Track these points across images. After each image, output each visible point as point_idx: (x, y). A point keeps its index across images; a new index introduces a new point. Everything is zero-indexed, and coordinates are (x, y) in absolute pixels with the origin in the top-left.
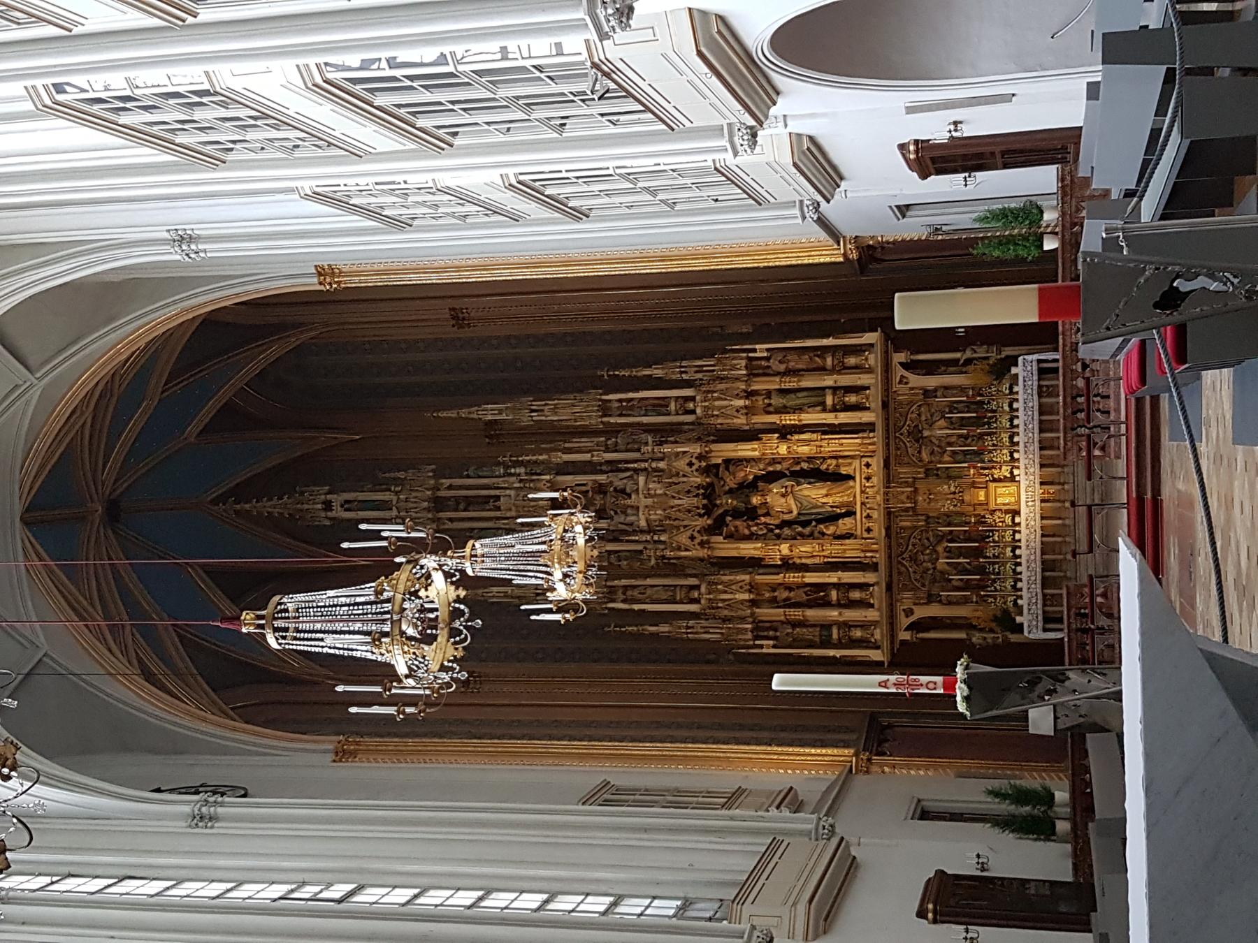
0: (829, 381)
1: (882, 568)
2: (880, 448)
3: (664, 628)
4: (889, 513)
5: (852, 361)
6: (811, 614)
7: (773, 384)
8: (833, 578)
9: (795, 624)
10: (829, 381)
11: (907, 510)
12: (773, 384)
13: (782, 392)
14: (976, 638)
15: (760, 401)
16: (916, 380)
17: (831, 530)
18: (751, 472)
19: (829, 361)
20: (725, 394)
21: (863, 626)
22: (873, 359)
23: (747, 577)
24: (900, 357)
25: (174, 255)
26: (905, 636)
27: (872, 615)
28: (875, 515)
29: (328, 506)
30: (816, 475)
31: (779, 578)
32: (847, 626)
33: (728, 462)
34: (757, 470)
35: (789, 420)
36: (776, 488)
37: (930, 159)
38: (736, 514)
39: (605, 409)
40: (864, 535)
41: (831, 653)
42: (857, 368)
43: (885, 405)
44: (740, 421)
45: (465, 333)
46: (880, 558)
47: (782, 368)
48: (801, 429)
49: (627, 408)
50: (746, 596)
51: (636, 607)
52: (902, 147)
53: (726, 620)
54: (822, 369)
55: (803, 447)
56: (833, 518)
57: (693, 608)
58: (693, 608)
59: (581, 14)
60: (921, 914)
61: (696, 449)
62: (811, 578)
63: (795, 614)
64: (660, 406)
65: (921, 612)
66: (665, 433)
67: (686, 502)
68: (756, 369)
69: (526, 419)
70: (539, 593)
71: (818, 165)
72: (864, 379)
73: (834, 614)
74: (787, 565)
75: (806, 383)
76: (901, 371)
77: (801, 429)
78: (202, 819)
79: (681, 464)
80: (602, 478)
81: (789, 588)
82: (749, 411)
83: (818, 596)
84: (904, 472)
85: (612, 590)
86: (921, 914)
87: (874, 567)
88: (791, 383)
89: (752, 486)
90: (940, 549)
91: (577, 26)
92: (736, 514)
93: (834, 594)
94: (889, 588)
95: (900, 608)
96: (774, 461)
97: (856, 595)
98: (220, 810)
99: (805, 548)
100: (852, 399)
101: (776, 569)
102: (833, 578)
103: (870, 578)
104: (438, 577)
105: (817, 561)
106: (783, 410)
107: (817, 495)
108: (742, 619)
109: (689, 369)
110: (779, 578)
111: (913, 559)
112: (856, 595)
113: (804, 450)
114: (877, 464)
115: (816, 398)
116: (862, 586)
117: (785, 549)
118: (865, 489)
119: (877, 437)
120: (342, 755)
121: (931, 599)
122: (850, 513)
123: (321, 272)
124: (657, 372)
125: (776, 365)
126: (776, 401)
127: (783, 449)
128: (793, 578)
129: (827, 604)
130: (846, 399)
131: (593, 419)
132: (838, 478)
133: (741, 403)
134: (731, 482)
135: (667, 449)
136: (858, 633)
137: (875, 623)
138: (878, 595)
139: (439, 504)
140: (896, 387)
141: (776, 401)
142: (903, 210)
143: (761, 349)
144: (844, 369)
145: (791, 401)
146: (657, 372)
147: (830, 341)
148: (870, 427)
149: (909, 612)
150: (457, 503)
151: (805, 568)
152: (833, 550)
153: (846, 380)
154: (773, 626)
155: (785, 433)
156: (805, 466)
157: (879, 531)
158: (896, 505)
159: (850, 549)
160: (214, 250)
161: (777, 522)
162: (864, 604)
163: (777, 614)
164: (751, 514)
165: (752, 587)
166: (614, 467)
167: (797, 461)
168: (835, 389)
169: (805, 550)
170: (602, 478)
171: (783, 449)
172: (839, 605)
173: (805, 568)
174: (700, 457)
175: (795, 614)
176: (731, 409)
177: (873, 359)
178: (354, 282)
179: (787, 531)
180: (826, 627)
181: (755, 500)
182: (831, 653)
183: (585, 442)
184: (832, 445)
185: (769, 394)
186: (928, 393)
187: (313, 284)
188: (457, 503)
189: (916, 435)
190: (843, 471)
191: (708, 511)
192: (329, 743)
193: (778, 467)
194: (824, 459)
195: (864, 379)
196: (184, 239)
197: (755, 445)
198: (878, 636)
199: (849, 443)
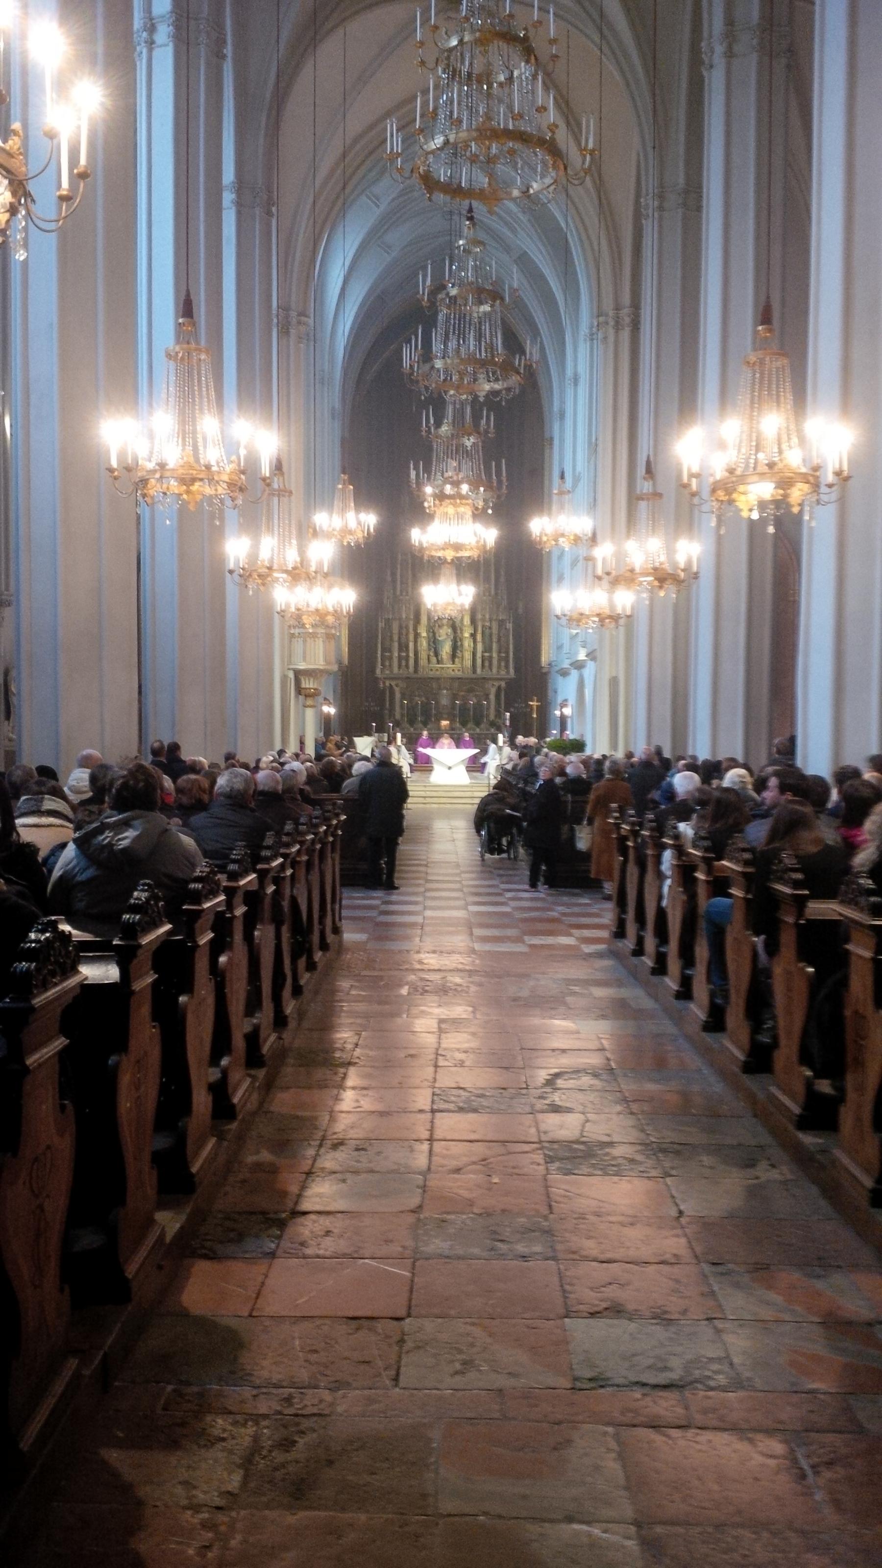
0: (495, 655)
1: (415, 676)
3: (389, 579)
4: (438, 679)
5: (503, 664)
6: (396, 645)
8: (411, 654)
10: (495, 655)
11: (440, 686)
12: (495, 631)
13: (491, 635)
16: (493, 691)
17: (432, 654)
19: (503, 655)
24: (503, 684)
25: (556, 409)
26: (387, 684)
27: (396, 670)
28: (438, 673)
31: (411, 630)
32: (391, 658)
35: (479, 637)
36: (450, 631)
41: (379, 652)
42: (499, 667)
43: (484, 678)
47: (501, 635)
50: (404, 617)
51: (399, 566)
54: (499, 652)
55: (467, 643)
56: (436, 654)
58: (398, 593)
62: (411, 645)
63: (396, 638)
65: (397, 691)
68: (501, 623)
71: (564, 673)
72: (495, 670)
74: (417, 635)
75: (495, 646)
76: (496, 684)
77: (475, 642)
81: (407, 634)
82: (483, 620)
83: (404, 647)
84: (456, 684)
87: (416, 670)
88: (495, 639)
90: (423, 699)
93: (404, 654)
94: (408, 678)
95: (399, 682)
96: (461, 630)
97: (404, 663)
99: (425, 643)
100: (487, 664)
101: (415, 629)
102: (411, 654)
103: (411, 669)
105: (419, 648)
107: (446, 649)
108: (393, 614)
110: (411, 630)
112: (404, 663)
114: (459, 674)
115: (488, 649)
116: (407, 666)
117: (424, 634)
118: (449, 668)
119: (469, 674)
120: (343, 441)
123: (552, 439)
127: (467, 635)
128: (411, 637)
130: (487, 661)
132: (453, 656)
133: (487, 616)
137: (391, 671)
140: (491, 682)
143: (509, 626)
144: (499, 661)
147: (511, 647)
148: (474, 671)
149: (397, 685)
151: (416, 642)
152: (423, 655)
153: (495, 662)
155: (473, 636)
156: (459, 643)
157: (431, 674)
159: (423, 662)
161: (436, 630)
162: (400, 666)
163: (395, 630)
167: (461, 640)
168: (491, 657)
169: (424, 644)
172: (399, 656)
173: (416, 642)
175: (396, 638)
179: (431, 635)
180: (390, 651)
182: (379, 652)
184: (468, 656)
185: (490, 628)
187: (547, 435)
189: (470, 691)
190: (457, 660)
193: (459, 632)
194: (461, 651)
195: (495, 670)
197: (469, 623)
198: (387, 672)
199: (468, 663)
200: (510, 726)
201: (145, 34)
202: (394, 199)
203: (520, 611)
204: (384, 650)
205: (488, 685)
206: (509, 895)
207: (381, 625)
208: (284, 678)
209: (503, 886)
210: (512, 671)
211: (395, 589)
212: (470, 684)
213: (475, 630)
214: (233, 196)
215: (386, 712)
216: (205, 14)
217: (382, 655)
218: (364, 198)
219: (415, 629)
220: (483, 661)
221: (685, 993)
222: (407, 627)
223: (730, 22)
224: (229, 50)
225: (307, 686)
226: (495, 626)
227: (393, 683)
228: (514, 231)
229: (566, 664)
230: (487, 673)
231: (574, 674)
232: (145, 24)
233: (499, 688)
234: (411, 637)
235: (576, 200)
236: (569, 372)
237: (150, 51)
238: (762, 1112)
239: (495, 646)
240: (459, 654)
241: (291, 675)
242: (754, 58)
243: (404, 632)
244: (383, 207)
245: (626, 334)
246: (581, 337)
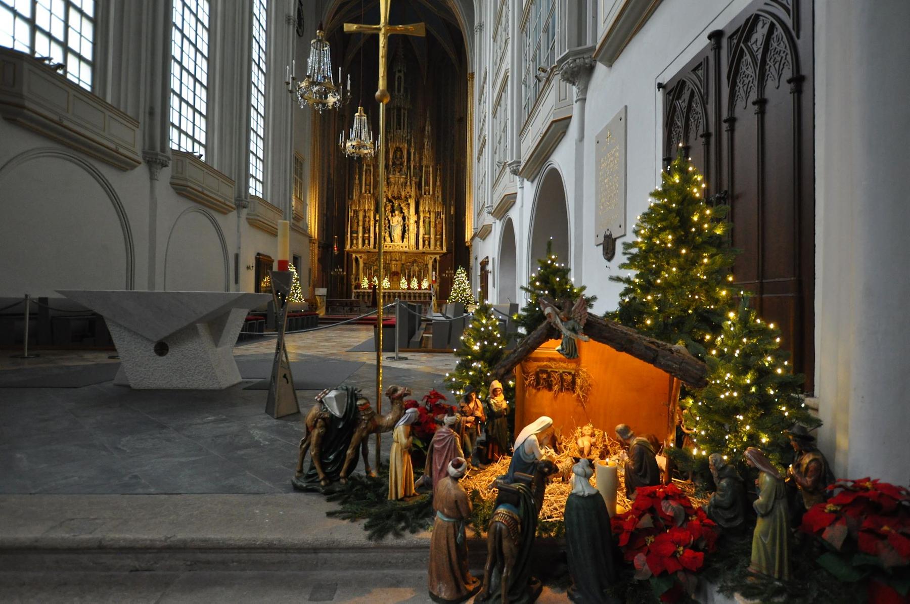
0: (432, 236)
3: (357, 182)
6: (361, 228)
8: (372, 235)
9: (358, 223)
10: (432, 236)
12: (432, 220)
15: (428, 215)
18: (405, 211)
21: (357, 244)
22: (438, 249)
24: (438, 257)
26: (354, 256)
29: (400, 71)
32: (357, 238)
33: (409, 204)
34: (406, 213)
36: (400, 219)
37: (484, 264)
38: (393, 206)
39: (427, 167)
44: (421, 209)
48: (418, 227)
49: (427, 173)
52: (487, 257)
55: (412, 227)
57: (363, 191)
58: (363, 191)
59: (515, 159)
60: (258, 254)
61: (413, 194)
63: (361, 223)
64: (427, 184)
65: (361, 261)
66: (419, 186)
67: (396, 191)
69: (426, 140)
70: (348, 137)
72: (432, 247)
73: (360, 235)
75: (432, 229)
76: (433, 257)
77: (418, 227)
78: (288, 19)
79: (408, 189)
80: (405, 164)
83: (366, 230)
84: (404, 257)
85: (369, 166)
86: (258, 254)
88: (432, 225)
89: (402, 212)
91: (512, 158)
92: (393, 206)
95: (362, 255)
97: (367, 242)
98: (291, 27)
100: (427, 243)
102: (372, 235)
103: (372, 246)
104: (335, 100)
106: (424, 221)
107: (397, 232)
109: (439, 193)
114: (406, 250)
119: (415, 250)
121: (365, 264)
123: (473, 74)
124: (438, 183)
126: (427, 220)
129: (364, 233)
131: (424, 163)
132: (403, 238)
134: (402, 205)
135: (414, 185)
138: (366, 248)
139: (399, 109)
141: (427, 220)
142: (476, 259)
143: (443, 216)
144: (436, 241)
145: (427, 225)
148: (418, 248)
150: (399, 115)
154: (357, 216)
155: (417, 222)
160: (477, 37)
163: (361, 218)
164: (393, 211)
165: (369, 210)
166: (409, 168)
170: (405, 164)
174: (410, 196)
175: (361, 223)
177: (438, 249)
178: (469, 85)
180: (357, 232)
181: (397, 212)
183: (417, 159)
187: (469, 71)
188: (399, 115)
189: (415, 261)
191: (394, 197)
195: (432, 247)
196: (481, 27)
203: (452, 212)
204: (352, 232)
205: (427, 258)
207: (351, 214)
213: (419, 218)
217: (351, 236)
220: (424, 241)
226: (433, 216)
230: (427, 249)
243: (367, 220)
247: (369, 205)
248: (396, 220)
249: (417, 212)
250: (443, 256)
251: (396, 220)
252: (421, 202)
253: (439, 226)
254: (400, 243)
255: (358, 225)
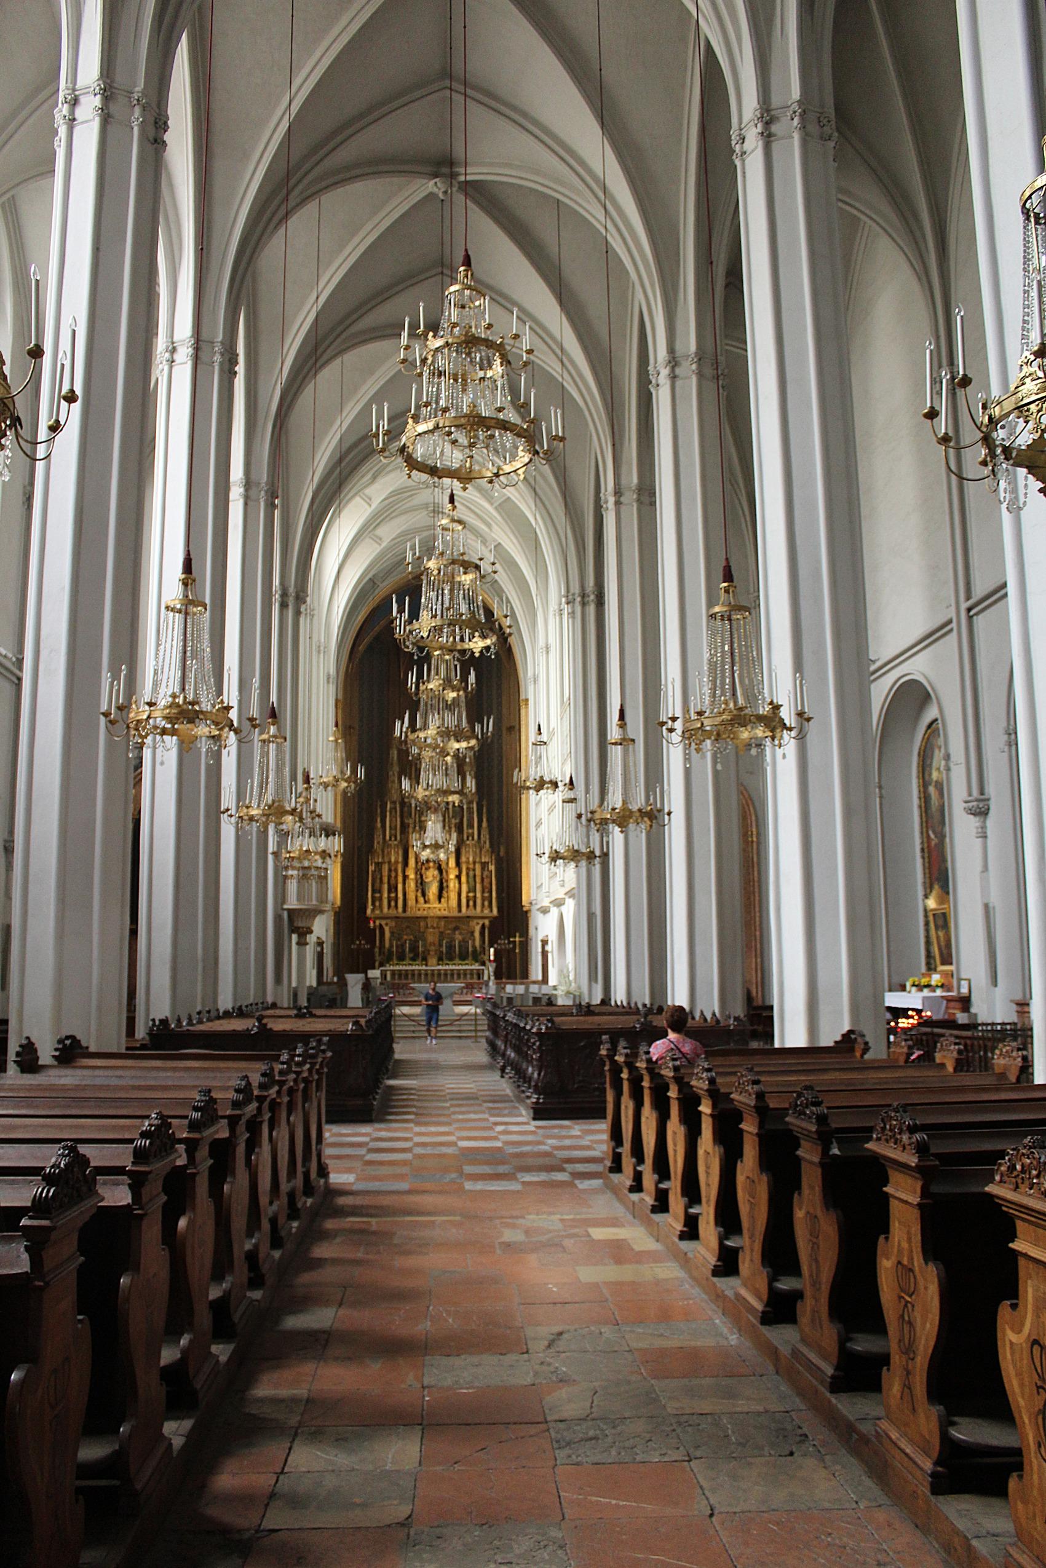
0: (479, 895)
1: (404, 915)
2: (452, 914)
3: (379, 825)
4: (426, 918)
5: (486, 903)
6: (386, 886)
7: (478, 872)
8: (400, 895)
10: (479, 895)
12: (478, 872)
13: (475, 876)
14: (377, 950)
15: (471, 866)
16: (478, 929)
17: (419, 894)
20: (475, 853)
22: (486, 912)
23: (400, 859)
24: (487, 922)
25: (530, 674)
26: (377, 922)
27: (385, 910)
30: (441, 889)
32: (381, 899)
35: (464, 879)
36: (436, 873)
40: (417, 908)
42: (483, 905)
44: (463, 859)
45: (504, 732)
46: (408, 914)
48: (460, 883)
49: (470, 809)
50: (393, 860)
53: (383, 851)
54: (483, 892)
55: (453, 884)
56: (424, 895)
57: (388, 838)
58: (388, 838)
62: (400, 887)
63: (385, 879)
66: (460, 831)
68: (484, 865)
72: (479, 908)
73: (386, 895)
74: (405, 877)
75: (478, 887)
76: (481, 922)
77: (460, 883)
81: (396, 877)
83: (393, 888)
84: (443, 923)
87: (404, 911)
88: (478, 879)
93: (393, 895)
95: (388, 921)
97: (393, 903)
100: (471, 903)
101: (404, 872)
102: (400, 895)
103: (400, 909)
107: (433, 890)
111: (408, 927)
112: (393, 903)
113: (451, 885)
114: (445, 913)
116: (396, 906)
117: (412, 876)
118: (436, 908)
119: (456, 914)
120: (337, 701)
121: (392, 933)
122: (426, 902)
123: (527, 700)
124: (485, 824)
125: (486, 873)
126: (471, 873)
127: (452, 876)
128: (400, 879)
129: (389, 892)
132: (440, 897)
133: (471, 859)
136: (377, 904)
137: (382, 911)
138: (393, 912)
140: (475, 921)
141: (471, 873)
143: (492, 868)
145: (471, 880)
146: (485, 824)
147: (494, 887)
148: (460, 911)
151: (404, 883)
152: (411, 896)
153: (479, 901)
154: (380, 870)
155: (459, 877)
157: (419, 913)
158: (429, 920)
159: (411, 902)
160: (531, 689)
162: (389, 906)
163: (385, 872)
168: (475, 897)
169: (411, 885)
171: (452, 876)
172: (389, 897)
173: (404, 883)
175: (385, 879)
176: (468, 856)
177: (486, 912)
178: (523, 712)
180: (380, 891)
184: (453, 896)
185: (474, 870)
186: (472, 933)
187: (522, 697)
189: (456, 928)
192: (340, 697)
195: (479, 908)
199: (454, 902)
200: (494, 961)
201: (167, 355)
202: (385, 499)
203: (502, 854)
204: (374, 891)
205: (473, 923)
206: (499, 1128)
207: (372, 868)
208: (278, 918)
209: (493, 1119)
210: (495, 912)
211: (384, 835)
212: (457, 922)
213: (460, 872)
214: (242, 490)
215: (377, 950)
216: (220, 338)
217: (373, 897)
218: (357, 499)
219: (404, 872)
221: (691, 1231)
222: (396, 870)
223: (671, 350)
224: (240, 368)
225: (300, 925)
226: (478, 867)
227: (383, 922)
228: (489, 526)
229: (546, 903)
231: (554, 911)
232: (167, 347)
233: (483, 926)
234: (400, 879)
235: (544, 498)
236: (541, 642)
237: (171, 368)
238: (786, 1367)
239: (478, 887)
240: (445, 894)
241: (285, 914)
242: (694, 380)
243: (393, 874)
244: (374, 506)
245: (591, 609)
246: (551, 613)
247: (395, 856)
248: (431, 875)
249: (458, 864)
250: (494, 921)
251: (431, 875)
252: (463, 851)
253: (486, 881)
254: (437, 905)
255: (381, 881)
